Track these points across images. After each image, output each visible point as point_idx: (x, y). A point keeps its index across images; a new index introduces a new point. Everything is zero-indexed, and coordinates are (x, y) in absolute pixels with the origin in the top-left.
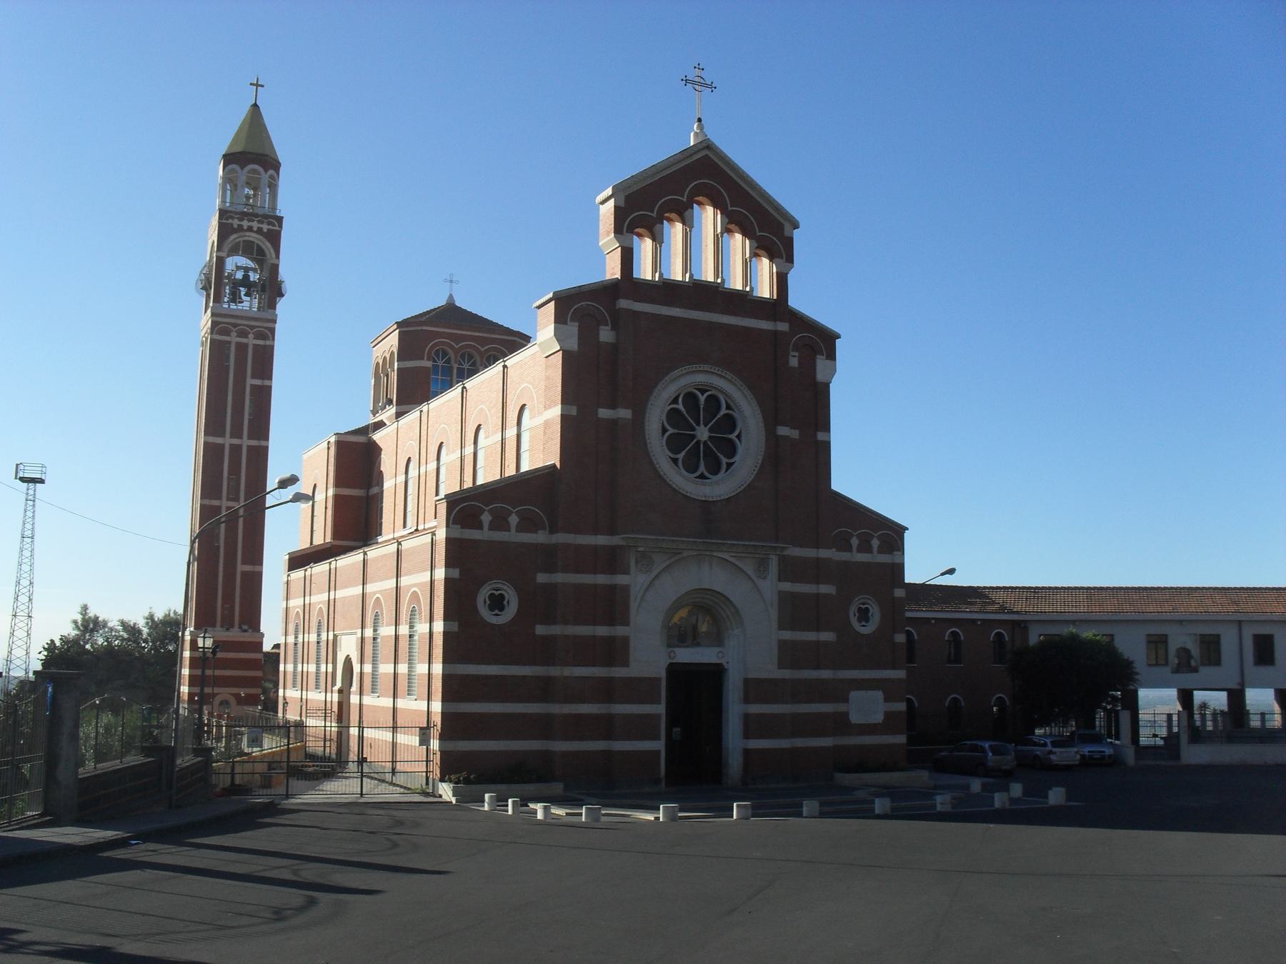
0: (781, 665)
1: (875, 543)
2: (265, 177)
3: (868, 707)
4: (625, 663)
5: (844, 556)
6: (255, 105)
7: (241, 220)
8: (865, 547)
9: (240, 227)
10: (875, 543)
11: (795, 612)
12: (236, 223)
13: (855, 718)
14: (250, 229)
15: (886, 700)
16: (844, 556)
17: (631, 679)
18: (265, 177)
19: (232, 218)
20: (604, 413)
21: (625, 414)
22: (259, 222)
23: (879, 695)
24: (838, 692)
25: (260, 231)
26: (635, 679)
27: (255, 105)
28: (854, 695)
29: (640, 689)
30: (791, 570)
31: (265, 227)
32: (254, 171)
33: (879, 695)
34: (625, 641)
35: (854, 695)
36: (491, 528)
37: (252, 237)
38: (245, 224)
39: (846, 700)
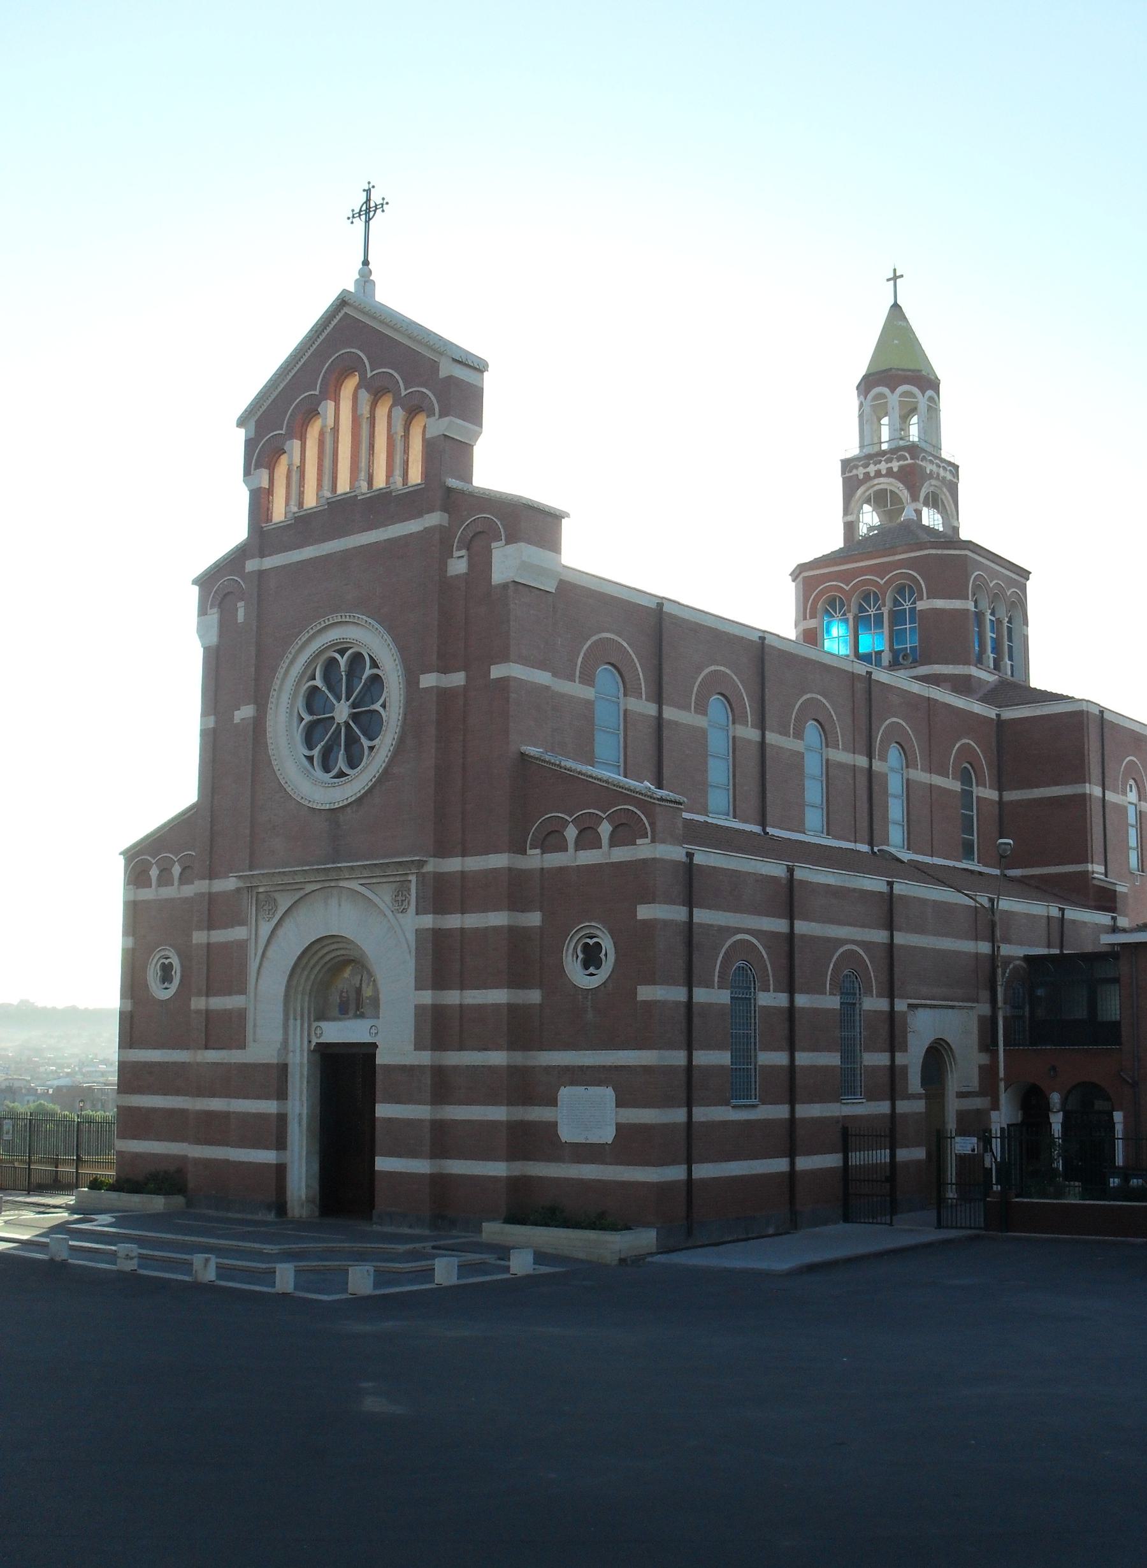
0: (419, 1046)
1: (605, 829)
2: (922, 401)
3: (587, 1115)
4: (242, 1046)
5: (555, 860)
6: (896, 307)
7: (866, 466)
8: (588, 838)
9: (867, 474)
10: (605, 829)
11: (442, 960)
12: (860, 472)
13: (567, 1134)
14: (878, 474)
15: (619, 1104)
16: (555, 860)
17: (245, 1065)
18: (922, 401)
19: (856, 467)
20: (458, 679)
21: (428, 680)
22: (887, 461)
23: (607, 1094)
24: (527, 1087)
25: (890, 473)
26: (250, 1064)
27: (896, 307)
28: (566, 1093)
29: (274, 1079)
30: (441, 895)
31: (895, 466)
32: (881, 396)
33: (607, 1094)
34: (240, 1016)
35: (566, 1093)
36: (613, 844)
37: (885, 483)
38: (872, 469)
39: (553, 1102)
